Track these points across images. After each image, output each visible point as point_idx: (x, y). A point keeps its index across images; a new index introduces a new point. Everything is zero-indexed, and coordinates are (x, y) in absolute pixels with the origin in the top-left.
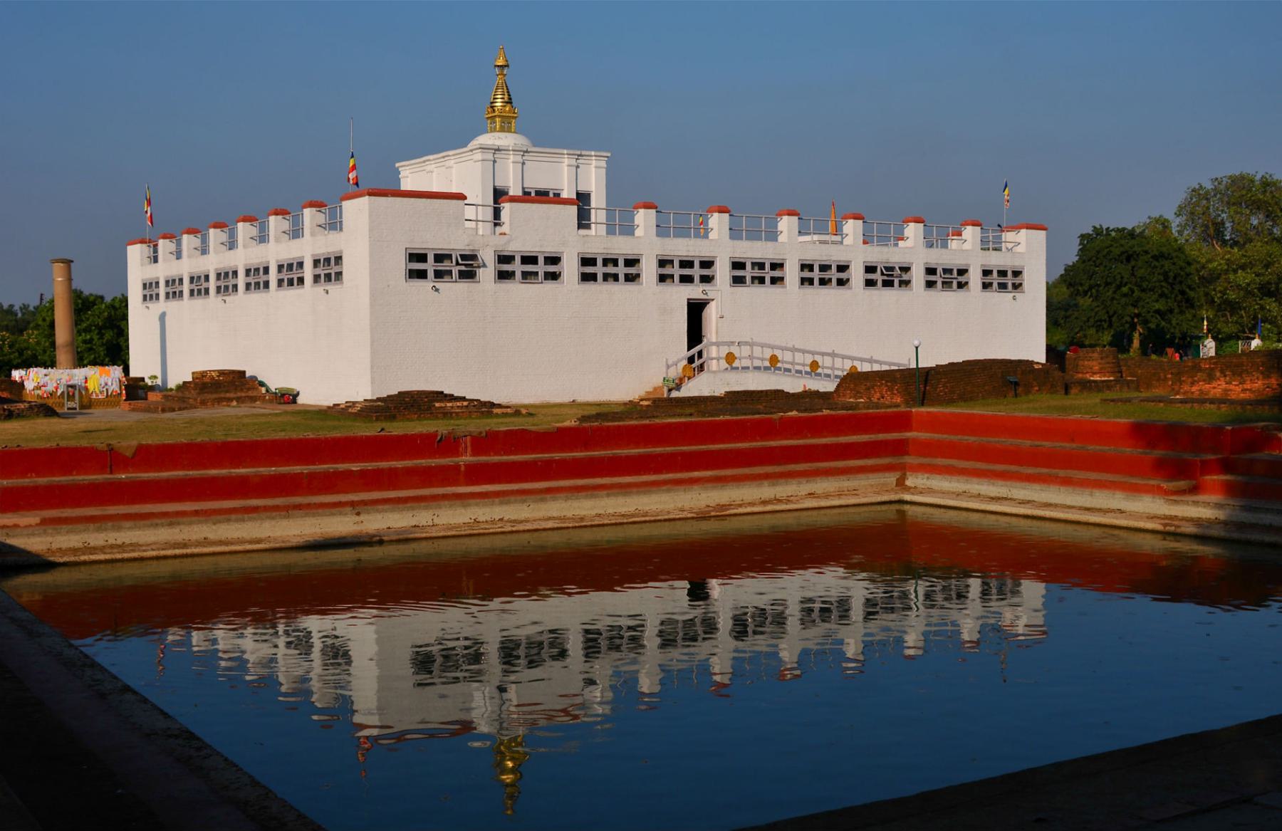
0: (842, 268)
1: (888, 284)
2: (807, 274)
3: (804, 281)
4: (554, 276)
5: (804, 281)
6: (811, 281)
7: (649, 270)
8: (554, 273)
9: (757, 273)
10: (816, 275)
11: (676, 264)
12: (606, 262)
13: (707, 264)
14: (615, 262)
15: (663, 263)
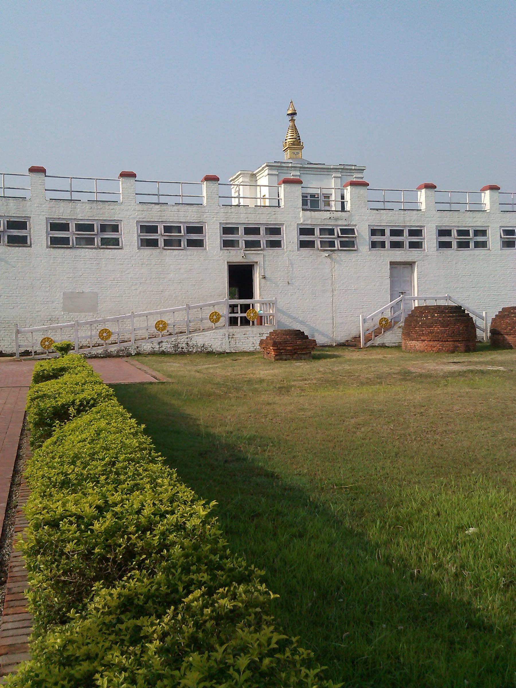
0: (416, 232)
1: (463, 245)
2: (377, 238)
3: (374, 245)
4: (116, 242)
5: (374, 245)
6: (383, 245)
7: (212, 237)
8: (232, 241)
9: (327, 237)
10: (387, 238)
11: (241, 231)
12: (168, 229)
13: (275, 231)
14: (179, 229)
15: (227, 230)
